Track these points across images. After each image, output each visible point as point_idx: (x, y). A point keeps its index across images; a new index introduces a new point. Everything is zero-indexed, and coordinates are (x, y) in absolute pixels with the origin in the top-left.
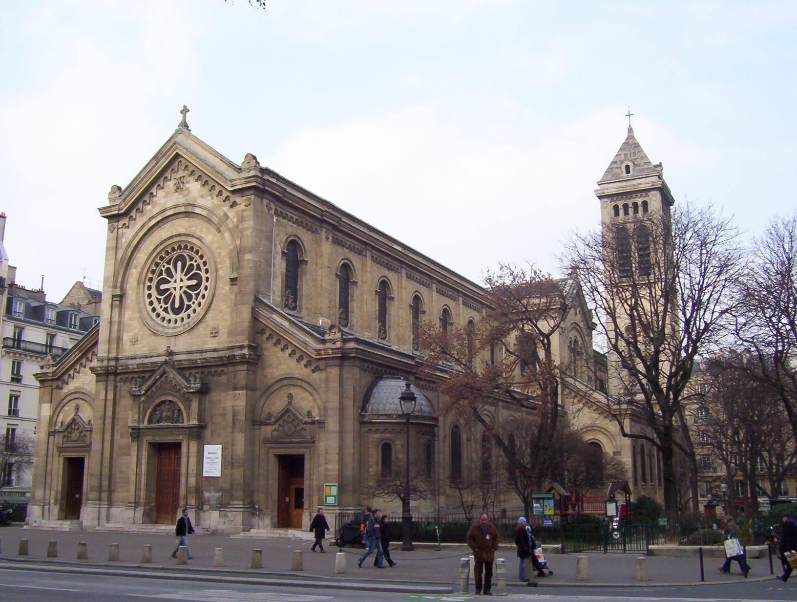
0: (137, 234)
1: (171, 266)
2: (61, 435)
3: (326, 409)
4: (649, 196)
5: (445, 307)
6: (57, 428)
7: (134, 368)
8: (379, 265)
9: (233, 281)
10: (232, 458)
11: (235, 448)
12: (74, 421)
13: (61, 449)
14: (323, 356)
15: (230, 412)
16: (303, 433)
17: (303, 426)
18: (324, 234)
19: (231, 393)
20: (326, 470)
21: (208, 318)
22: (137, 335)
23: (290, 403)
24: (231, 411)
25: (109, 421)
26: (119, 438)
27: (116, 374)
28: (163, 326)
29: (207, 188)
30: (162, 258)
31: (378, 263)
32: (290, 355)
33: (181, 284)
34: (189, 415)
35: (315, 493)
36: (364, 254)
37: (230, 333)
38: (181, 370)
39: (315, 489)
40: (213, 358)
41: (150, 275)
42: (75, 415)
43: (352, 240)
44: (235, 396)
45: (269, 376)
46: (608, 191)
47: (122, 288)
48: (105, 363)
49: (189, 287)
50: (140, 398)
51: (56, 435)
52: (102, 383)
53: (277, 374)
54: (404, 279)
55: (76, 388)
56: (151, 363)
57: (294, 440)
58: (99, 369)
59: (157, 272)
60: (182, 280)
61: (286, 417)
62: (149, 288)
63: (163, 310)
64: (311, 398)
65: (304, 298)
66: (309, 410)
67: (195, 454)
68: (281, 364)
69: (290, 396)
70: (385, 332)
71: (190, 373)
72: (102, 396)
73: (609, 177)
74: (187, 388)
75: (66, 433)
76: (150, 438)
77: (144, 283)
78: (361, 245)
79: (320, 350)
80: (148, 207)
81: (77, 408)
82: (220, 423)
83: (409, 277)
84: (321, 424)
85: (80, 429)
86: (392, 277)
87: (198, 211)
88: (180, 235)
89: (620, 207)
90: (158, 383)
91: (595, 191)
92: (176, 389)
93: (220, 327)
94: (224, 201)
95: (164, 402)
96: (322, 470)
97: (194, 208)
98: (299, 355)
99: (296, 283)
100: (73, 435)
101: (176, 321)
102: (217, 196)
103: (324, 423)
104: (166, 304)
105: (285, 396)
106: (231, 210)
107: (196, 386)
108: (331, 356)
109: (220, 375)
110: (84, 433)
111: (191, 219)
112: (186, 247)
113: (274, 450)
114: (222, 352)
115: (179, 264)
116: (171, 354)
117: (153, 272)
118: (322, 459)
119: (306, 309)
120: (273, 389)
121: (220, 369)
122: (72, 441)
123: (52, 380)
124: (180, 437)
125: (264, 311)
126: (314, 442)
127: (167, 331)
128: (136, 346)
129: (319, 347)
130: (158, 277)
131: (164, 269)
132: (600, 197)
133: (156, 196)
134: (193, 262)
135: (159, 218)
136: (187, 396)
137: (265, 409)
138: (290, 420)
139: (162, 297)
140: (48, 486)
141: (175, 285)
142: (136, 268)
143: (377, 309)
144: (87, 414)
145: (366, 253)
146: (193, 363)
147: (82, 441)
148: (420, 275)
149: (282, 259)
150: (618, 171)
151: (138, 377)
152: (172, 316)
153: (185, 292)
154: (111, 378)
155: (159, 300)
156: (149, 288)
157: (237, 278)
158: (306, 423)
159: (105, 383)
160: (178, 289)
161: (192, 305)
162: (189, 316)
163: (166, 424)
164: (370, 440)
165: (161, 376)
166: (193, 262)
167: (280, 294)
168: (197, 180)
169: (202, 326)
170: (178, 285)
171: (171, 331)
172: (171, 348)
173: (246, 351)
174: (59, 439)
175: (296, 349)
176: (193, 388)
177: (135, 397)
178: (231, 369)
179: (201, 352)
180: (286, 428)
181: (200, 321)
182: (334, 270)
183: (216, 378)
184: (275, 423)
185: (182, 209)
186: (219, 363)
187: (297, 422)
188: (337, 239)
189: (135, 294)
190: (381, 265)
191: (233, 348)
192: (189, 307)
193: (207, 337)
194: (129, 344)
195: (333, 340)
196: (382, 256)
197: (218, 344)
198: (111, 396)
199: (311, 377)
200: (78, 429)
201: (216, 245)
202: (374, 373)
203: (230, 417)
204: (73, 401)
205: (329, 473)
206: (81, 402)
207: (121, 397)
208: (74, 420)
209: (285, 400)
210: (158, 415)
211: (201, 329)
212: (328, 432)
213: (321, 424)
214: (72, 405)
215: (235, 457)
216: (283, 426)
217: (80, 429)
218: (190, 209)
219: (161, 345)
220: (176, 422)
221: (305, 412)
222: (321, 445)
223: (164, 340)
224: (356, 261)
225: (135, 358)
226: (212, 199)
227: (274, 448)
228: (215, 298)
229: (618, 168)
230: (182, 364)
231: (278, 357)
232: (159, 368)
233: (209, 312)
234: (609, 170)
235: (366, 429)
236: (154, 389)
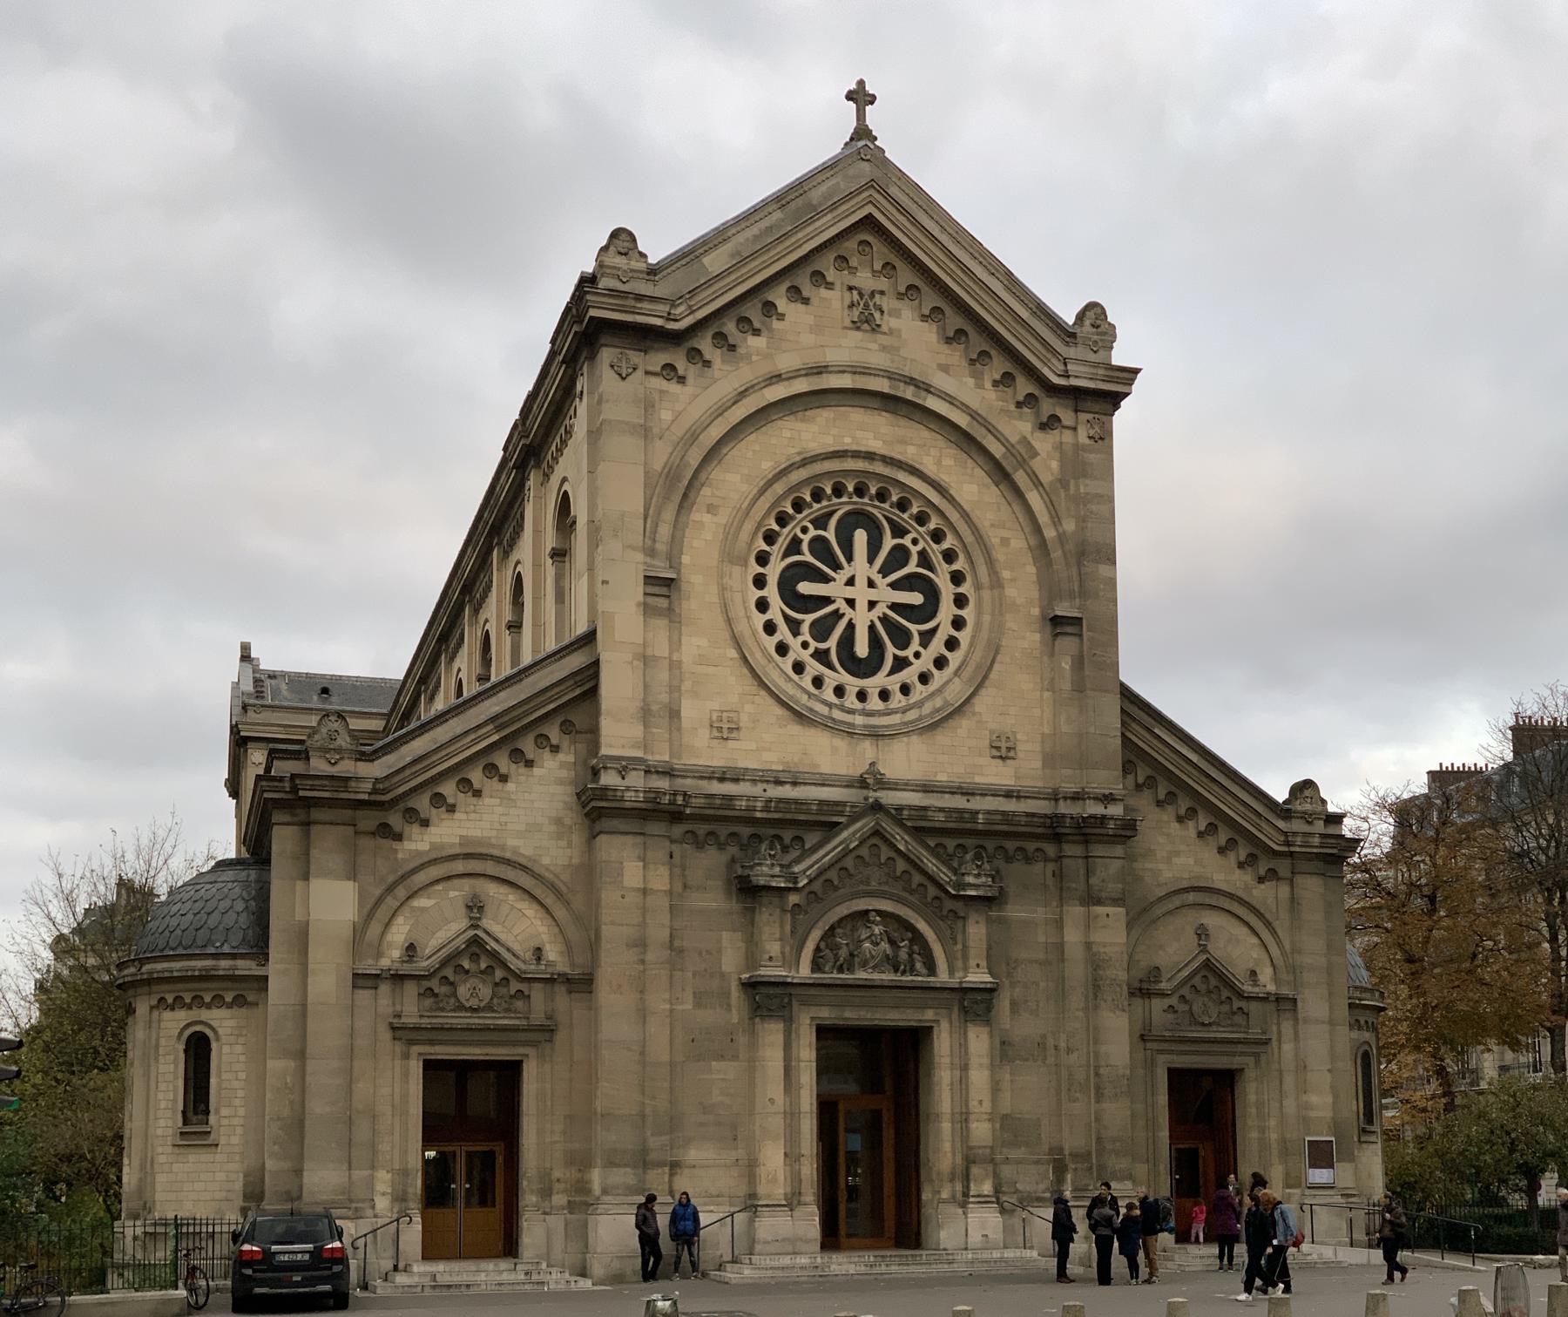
0: (722, 411)
1: (830, 535)
3: (1293, 969)
9: (1058, 624)
10: (1097, 1074)
11: (1103, 1049)
12: (475, 946)
17: (1243, 1004)
21: (981, 704)
26: (689, 1006)
27: (676, 816)
28: (830, 705)
29: (955, 356)
30: (798, 506)
33: (873, 595)
35: (1275, 1159)
37: (1050, 760)
40: (1028, 815)
47: (673, 560)
48: (636, 780)
52: (629, 839)
55: (465, 840)
56: (821, 803)
57: (1219, 1035)
59: (782, 542)
60: (871, 584)
62: (760, 582)
63: (812, 656)
64: (1255, 940)
75: (434, 984)
76: (826, 1014)
77: (745, 564)
79: (1295, 834)
81: (475, 907)
82: (1037, 985)
84: (1285, 1004)
87: (933, 403)
88: (870, 456)
93: (1019, 736)
94: (1019, 405)
96: (1290, 1105)
97: (923, 394)
100: (463, 991)
101: (862, 696)
102: (996, 383)
103: (1295, 1001)
104: (824, 640)
106: (1039, 434)
108: (1315, 850)
109: (1028, 860)
110: (515, 986)
111: (903, 422)
112: (882, 496)
113: (1169, 1057)
114: (1029, 801)
115: (860, 537)
117: (770, 538)
120: (1159, 911)
122: (462, 1008)
124: (929, 1015)
126: (1267, 1042)
129: (1281, 824)
130: (785, 555)
131: (806, 538)
134: (907, 541)
135: (801, 386)
136: (949, 904)
139: (809, 618)
141: (849, 592)
142: (711, 509)
146: (961, 820)
147: (508, 1010)
152: (853, 683)
155: (794, 627)
156: (760, 582)
157: (1081, 619)
158: (1249, 998)
159: (639, 839)
161: (912, 658)
162: (905, 689)
163: (876, 976)
166: (907, 541)
168: (924, 318)
169: (964, 725)
170: (861, 593)
171: (859, 720)
177: (748, 892)
178: (1071, 849)
179: (968, 792)
181: (959, 710)
183: (1017, 867)
185: (882, 385)
186: (1040, 830)
189: (714, 589)
191: (1077, 797)
192: (900, 664)
193: (980, 755)
194: (704, 733)
201: (990, 516)
204: (456, 882)
206: (492, 890)
207: (685, 886)
211: (962, 732)
214: (457, 893)
215: (1102, 1071)
217: (499, 974)
218: (908, 393)
220: (904, 973)
223: (841, 743)
225: (736, 780)
226: (980, 386)
227: (1171, 1052)
228: (999, 658)
230: (924, 818)
232: (854, 819)
233: (983, 692)
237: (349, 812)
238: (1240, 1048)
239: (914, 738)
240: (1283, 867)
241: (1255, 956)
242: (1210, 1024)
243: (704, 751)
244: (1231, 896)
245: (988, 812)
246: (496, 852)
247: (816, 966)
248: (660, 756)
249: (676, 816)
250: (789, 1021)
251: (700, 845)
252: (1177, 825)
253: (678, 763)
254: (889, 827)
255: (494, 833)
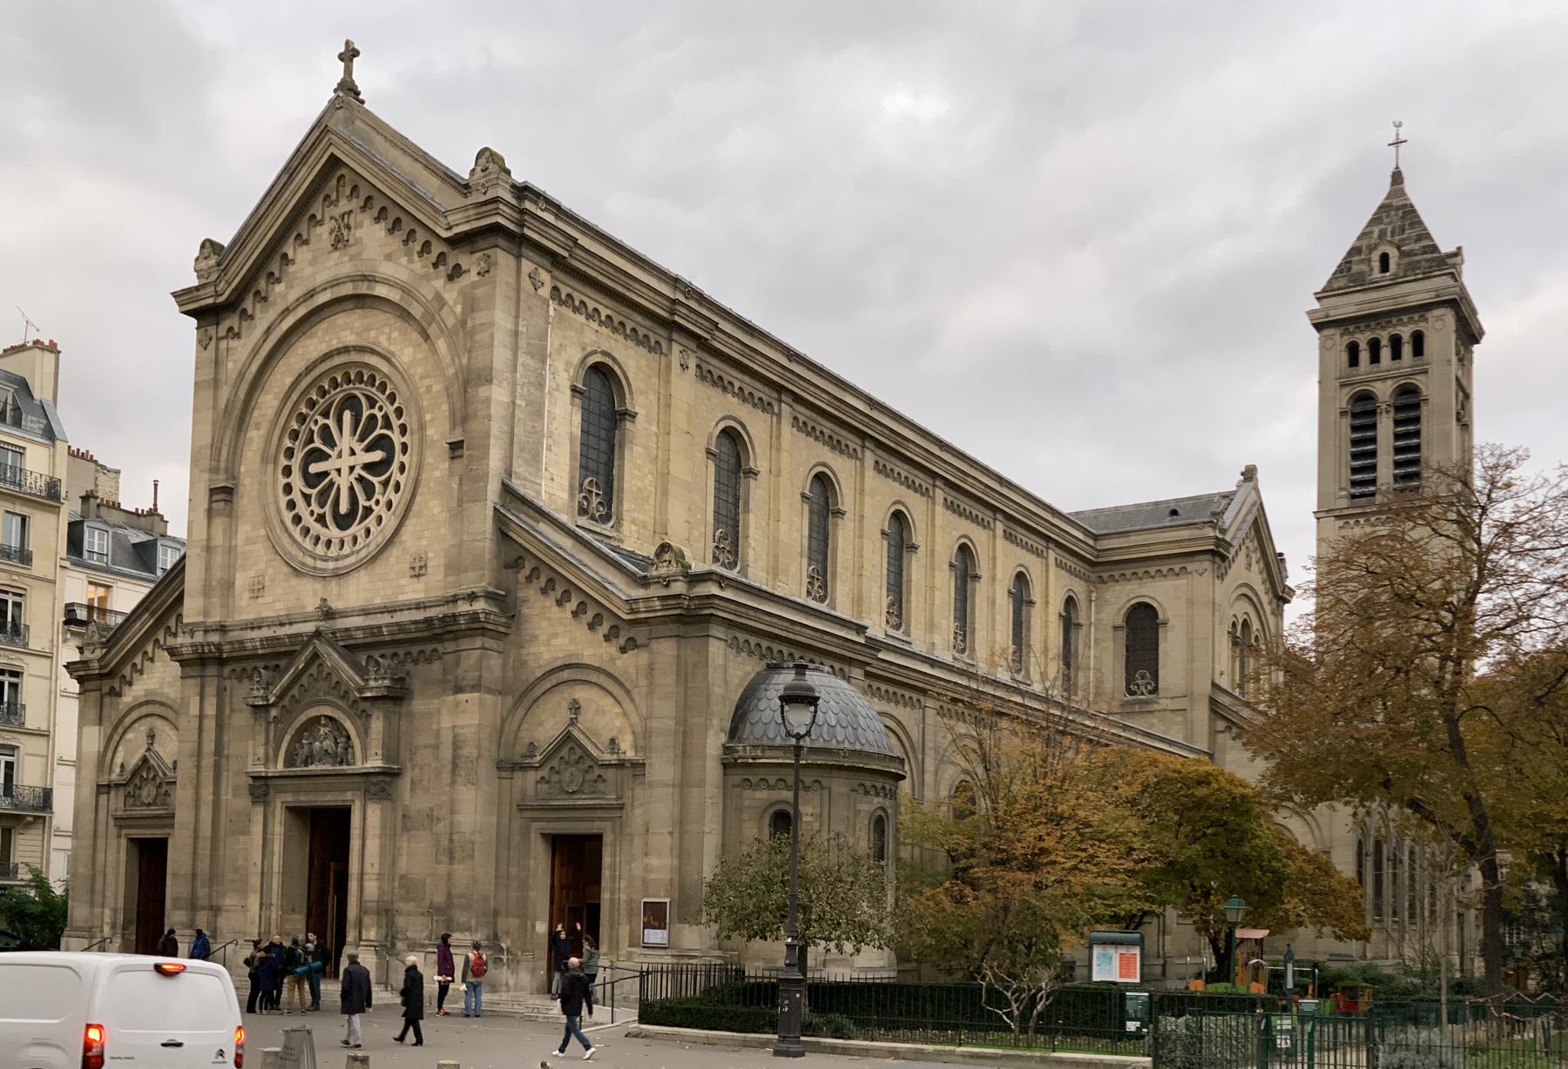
2: (122, 792)
3: (647, 733)
4: (1426, 320)
5: (963, 540)
6: (114, 777)
7: (255, 648)
8: (811, 440)
13: (121, 822)
14: (643, 615)
15: (447, 739)
16: (601, 786)
18: (675, 358)
19: (450, 699)
20: (647, 869)
21: (407, 534)
22: (263, 576)
23: (573, 722)
24: (450, 739)
25: (208, 761)
27: (221, 662)
31: (808, 434)
32: (575, 614)
34: (365, 749)
36: (776, 410)
38: (351, 648)
39: (623, 912)
41: (288, 443)
42: (149, 750)
43: (747, 379)
44: (457, 704)
45: (532, 664)
46: (1338, 311)
48: (199, 637)
49: (368, 467)
50: (267, 712)
51: (113, 793)
53: (547, 656)
54: (870, 472)
55: (148, 692)
56: (289, 636)
58: (184, 650)
61: (564, 752)
64: (618, 710)
65: (626, 496)
66: (613, 734)
67: (377, 832)
68: (555, 635)
69: (575, 707)
70: (824, 586)
71: (369, 657)
72: (194, 709)
73: (1342, 282)
74: (361, 690)
75: (131, 789)
78: (767, 390)
79: (636, 600)
80: (279, 288)
81: (151, 736)
83: (880, 469)
84: (638, 767)
85: (158, 781)
86: (843, 469)
89: (1363, 346)
90: (305, 680)
91: (1309, 313)
92: (339, 689)
93: (430, 555)
95: (316, 720)
98: (591, 610)
99: (610, 464)
100: (145, 792)
105: (565, 705)
107: (377, 685)
108: (659, 614)
109: (429, 661)
116: (328, 614)
118: (638, 842)
119: (634, 521)
120: (538, 691)
121: (428, 648)
123: (101, 676)
125: (522, 516)
126: (621, 807)
127: (320, 564)
128: (260, 600)
129: (639, 593)
132: (1319, 327)
133: (293, 262)
136: (362, 705)
137: (523, 734)
138: (574, 757)
140: (98, 898)
143: (806, 533)
144: (169, 747)
145: (780, 410)
148: (906, 467)
149: (572, 404)
150: (1363, 267)
151: (266, 668)
153: (360, 479)
154: (212, 670)
159: (198, 680)
160: (345, 471)
164: (747, 803)
165: (308, 665)
167: (566, 483)
169: (395, 552)
172: (329, 603)
173: (480, 605)
174: (116, 802)
175: (587, 601)
176: (371, 689)
178: (450, 646)
180: (566, 776)
181: (389, 543)
182: (703, 444)
183: (422, 668)
184: (542, 764)
186: (426, 634)
187: (588, 762)
188: (710, 372)
190: (817, 439)
191: (454, 600)
194: (247, 595)
195: (664, 579)
196: (819, 419)
197: (426, 591)
198: (211, 709)
199: (619, 663)
200: (154, 778)
202: (762, 657)
203: (446, 752)
204: (143, 721)
205: (652, 876)
206: (159, 723)
207: (232, 710)
208: (145, 760)
209: (565, 715)
210: (306, 749)
211: (392, 560)
212: (650, 785)
213: (638, 767)
214: (142, 728)
216: (558, 773)
219: (309, 596)
221: (606, 738)
222: (637, 816)
224: (756, 425)
229: (1362, 261)
230: (350, 637)
231: (549, 619)
232: (305, 645)
234: (1344, 268)
235: (737, 779)
236: (295, 691)
237: (98, 682)
238: (599, 814)
239: (362, 572)
240: (640, 634)
241: (618, 724)
242: (574, 792)
243: (246, 609)
244: (598, 670)
245: (387, 625)
246: (158, 699)
247: (289, 762)
248: (215, 618)
249: (221, 662)
250: (266, 804)
251: (240, 679)
252: (556, 608)
253: (229, 622)
254: (323, 648)
255: (157, 686)
